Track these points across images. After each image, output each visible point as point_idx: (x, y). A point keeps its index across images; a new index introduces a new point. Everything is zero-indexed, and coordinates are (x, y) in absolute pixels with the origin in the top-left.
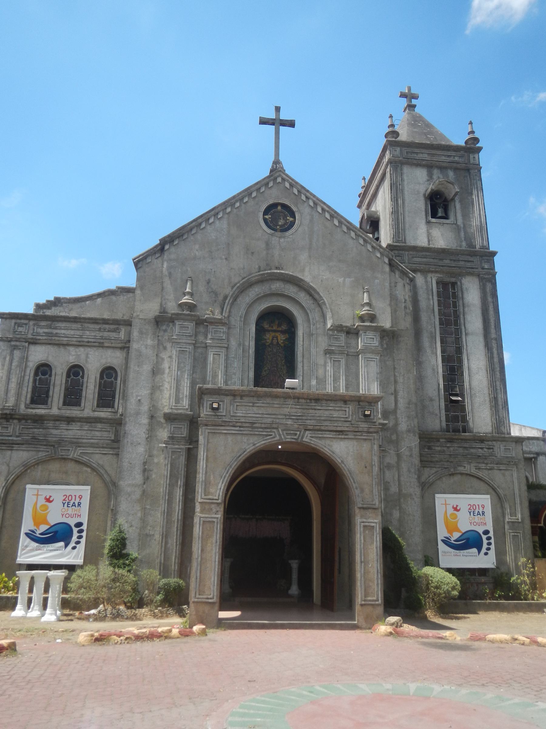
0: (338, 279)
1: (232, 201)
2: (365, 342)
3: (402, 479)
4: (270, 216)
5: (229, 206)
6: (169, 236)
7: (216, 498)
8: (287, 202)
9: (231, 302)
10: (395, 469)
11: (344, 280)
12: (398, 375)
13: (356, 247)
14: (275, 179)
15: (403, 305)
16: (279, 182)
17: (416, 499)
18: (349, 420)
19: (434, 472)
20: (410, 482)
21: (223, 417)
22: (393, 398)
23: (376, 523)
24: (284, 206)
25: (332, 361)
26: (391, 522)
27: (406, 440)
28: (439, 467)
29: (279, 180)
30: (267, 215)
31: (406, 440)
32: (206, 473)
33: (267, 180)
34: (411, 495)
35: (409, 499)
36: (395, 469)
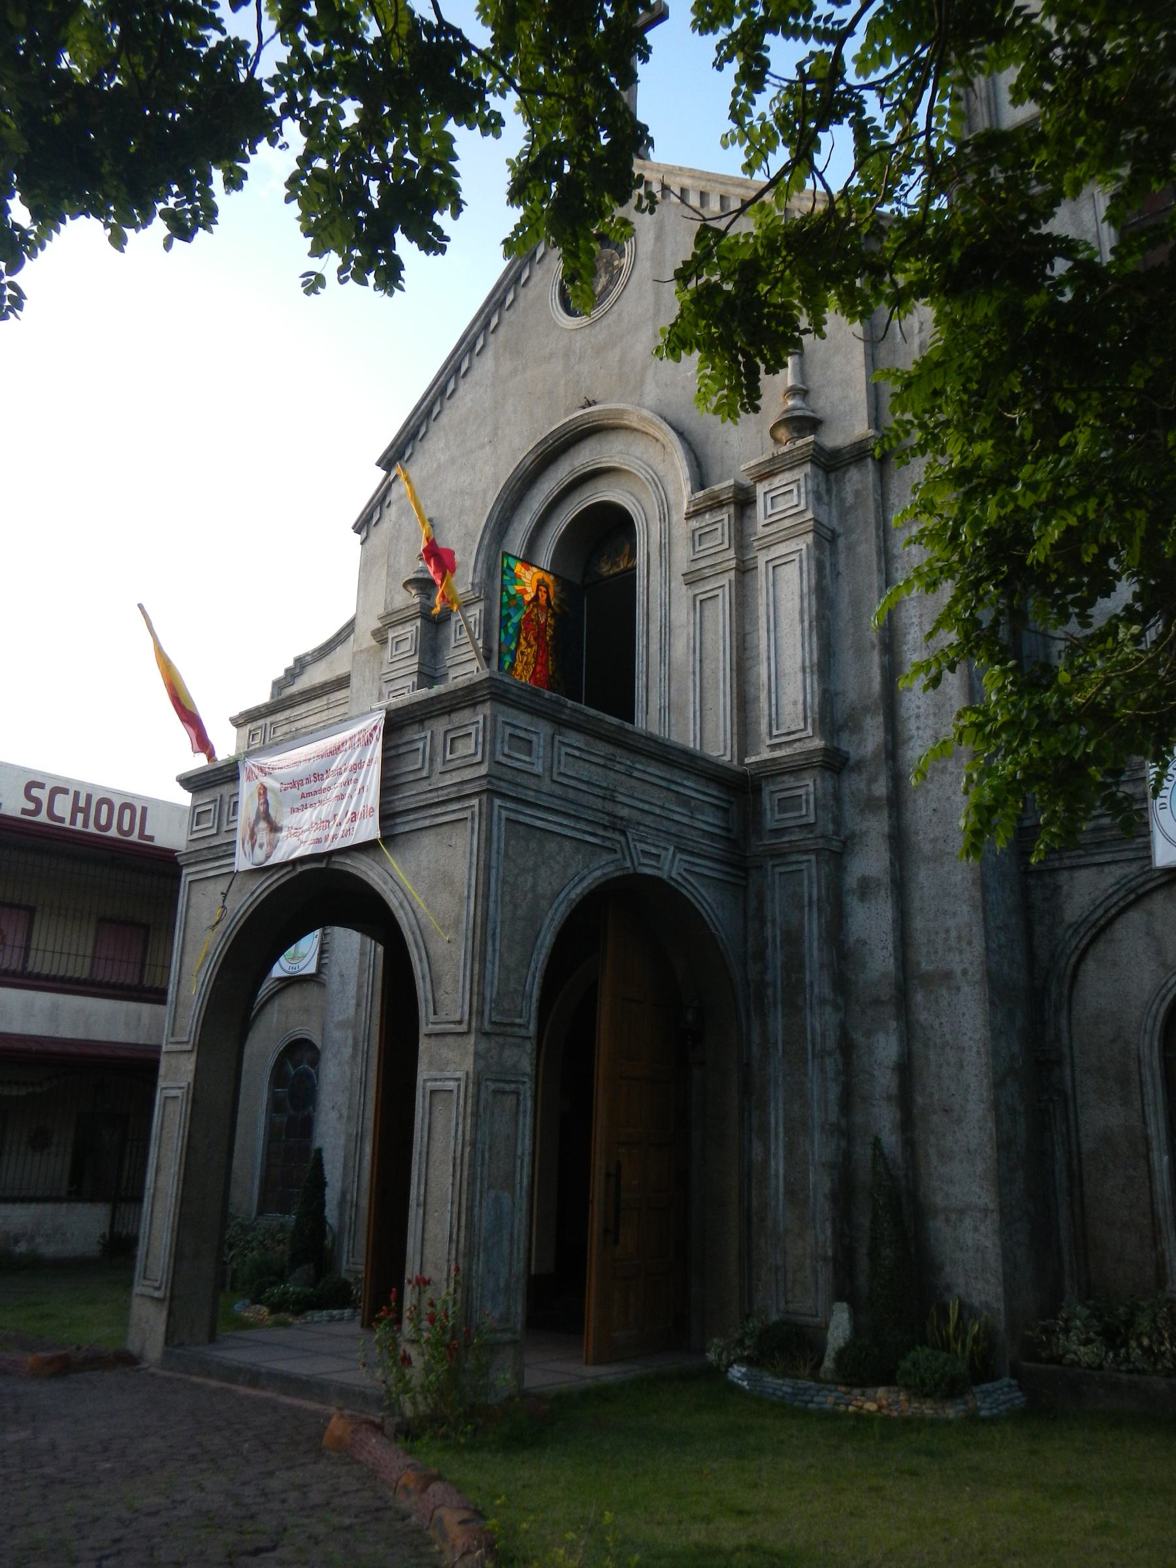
1: (497, 296)
2: (770, 512)
3: (918, 923)
6: (392, 446)
7: (185, 1039)
9: (486, 542)
10: (882, 893)
17: (966, 989)
18: (424, 773)
19: (1112, 880)
20: (947, 931)
21: (215, 838)
22: (875, 659)
23: (458, 1079)
26: (873, 1076)
27: (930, 786)
28: (1131, 860)
31: (930, 786)
32: (179, 982)
34: (948, 975)
35: (945, 992)
36: (882, 893)
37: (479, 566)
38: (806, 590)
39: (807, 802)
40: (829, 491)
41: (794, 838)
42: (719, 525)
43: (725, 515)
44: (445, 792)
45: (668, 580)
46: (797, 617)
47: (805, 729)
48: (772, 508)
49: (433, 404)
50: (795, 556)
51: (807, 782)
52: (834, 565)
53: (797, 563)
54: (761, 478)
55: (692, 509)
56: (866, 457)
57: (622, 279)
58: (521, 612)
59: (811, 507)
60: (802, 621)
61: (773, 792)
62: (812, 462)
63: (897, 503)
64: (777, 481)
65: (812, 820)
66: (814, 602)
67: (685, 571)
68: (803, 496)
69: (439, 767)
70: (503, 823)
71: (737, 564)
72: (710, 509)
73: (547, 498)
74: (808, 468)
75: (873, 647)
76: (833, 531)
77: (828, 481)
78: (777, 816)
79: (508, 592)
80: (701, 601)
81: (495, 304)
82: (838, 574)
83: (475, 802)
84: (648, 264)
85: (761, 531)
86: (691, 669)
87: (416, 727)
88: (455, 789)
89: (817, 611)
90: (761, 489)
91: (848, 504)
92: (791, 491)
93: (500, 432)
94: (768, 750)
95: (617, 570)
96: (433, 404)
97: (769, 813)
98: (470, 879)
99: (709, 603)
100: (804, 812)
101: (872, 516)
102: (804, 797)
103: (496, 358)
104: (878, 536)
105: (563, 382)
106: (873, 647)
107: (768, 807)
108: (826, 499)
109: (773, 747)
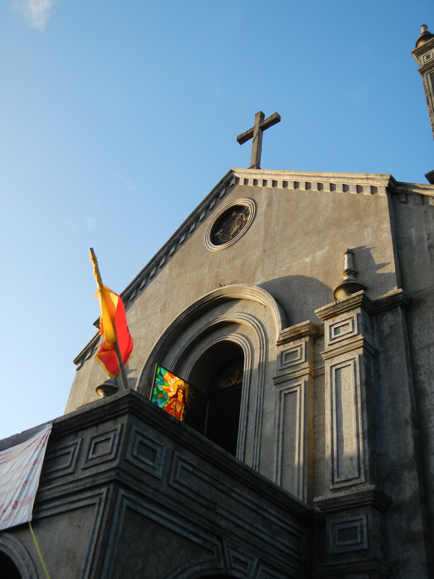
0: (304, 261)
1: (176, 238)
2: (333, 336)
4: (222, 230)
5: (173, 245)
8: (240, 202)
11: (314, 257)
12: (427, 380)
13: (333, 200)
14: (228, 183)
15: (426, 244)
16: (233, 185)
22: (409, 431)
24: (239, 209)
25: (283, 396)
29: (233, 182)
30: (219, 231)
33: (217, 191)
37: (144, 377)
38: (358, 383)
39: (362, 533)
40: (372, 327)
41: (350, 561)
42: (299, 349)
43: (303, 342)
44: (83, 482)
45: (263, 384)
46: (353, 400)
47: (359, 477)
48: (335, 334)
49: (131, 292)
50: (352, 362)
51: (361, 517)
52: (377, 371)
53: (352, 367)
54: (328, 317)
55: (281, 339)
56: (397, 306)
57: (247, 225)
58: (165, 402)
59: (361, 332)
60: (356, 403)
61: (334, 524)
62: (361, 306)
63: (418, 334)
64: (338, 319)
65: (365, 546)
66: (364, 391)
67: (275, 375)
68: (356, 326)
69: (82, 464)
70: (124, 509)
71: (310, 371)
72: (293, 339)
73: (191, 339)
74: (359, 310)
75: (407, 423)
76: (376, 350)
77: (371, 321)
78: (338, 543)
79: (157, 388)
80: (285, 395)
81: (174, 242)
82: (380, 376)
83: (104, 490)
84: (262, 217)
85: (327, 348)
86: (276, 439)
87: (72, 437)
88: (90, 480)
89: (366, 397)
90: (327, 324)
91: (385, 334)
92: (348, 324)
93: (167, 305)
94: (331, 493)
95: (230, 385)
96: (131, 292)
97: (331, 541)
98: (89, 554)
99: (291, 395)
100: (359, 540)
101: (403, 340)
102: (359, 529)
103: (171, 270)
104: (407, 353)
105: (207, 278)
106: (407, 423)
107: (331, 536)
108: (370, 331)
109: (335, 490)
